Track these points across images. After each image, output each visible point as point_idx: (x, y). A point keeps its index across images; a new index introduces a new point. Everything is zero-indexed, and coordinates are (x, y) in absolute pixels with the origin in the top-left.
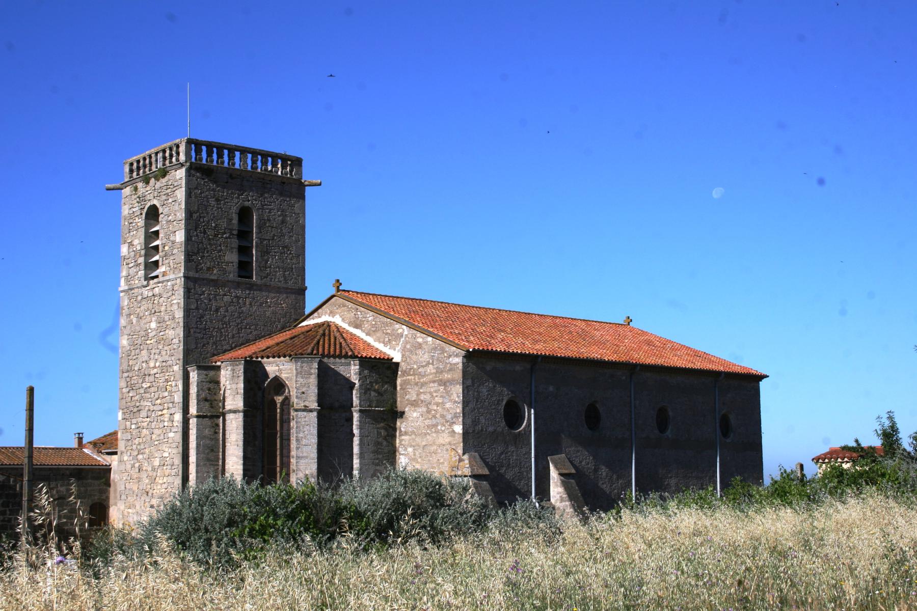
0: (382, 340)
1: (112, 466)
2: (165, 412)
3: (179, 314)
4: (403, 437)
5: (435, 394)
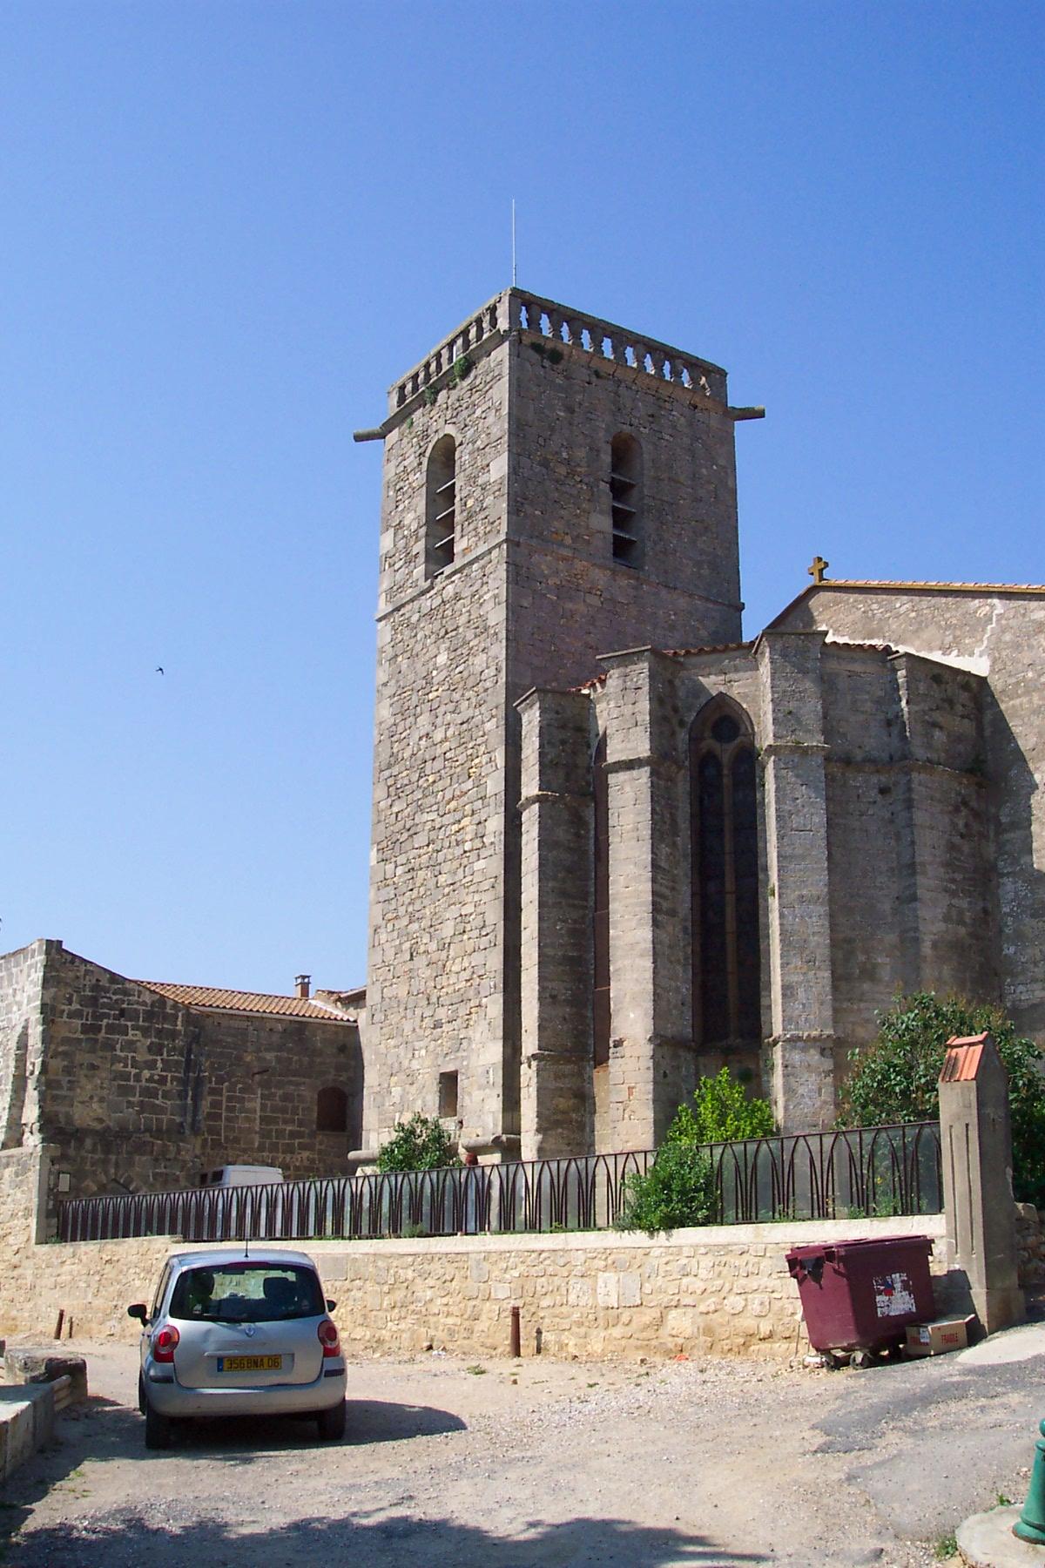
0: (938, 643)
1: (359, 1023)
2: (465, 822)
3: (497, 616)
4: (1007, 836)
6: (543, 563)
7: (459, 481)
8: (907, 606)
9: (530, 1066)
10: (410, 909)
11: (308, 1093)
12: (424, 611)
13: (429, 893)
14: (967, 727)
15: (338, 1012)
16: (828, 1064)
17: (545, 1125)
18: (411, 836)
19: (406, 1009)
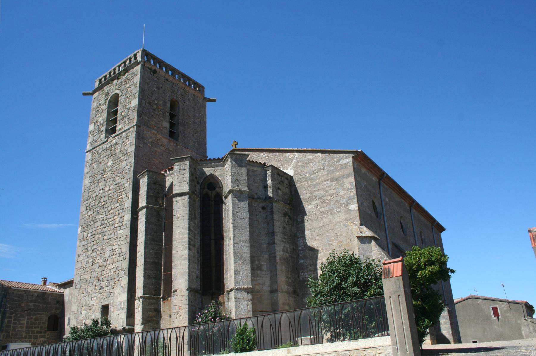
1: (65, 293)
3: (131, 149)
5: (328, 189)
6: (147, 134)
7: (120, 108)
8: (265, 155)
9: (139, 301)
10: (93, 248)
11: (44, 317)
12: (104, 148)
13: (100, 242)
14: (287, 191)
15: (57, 290)
16: (250, 297)
17: (145, 322)
18: (94, 223)
19: (89, 283)
